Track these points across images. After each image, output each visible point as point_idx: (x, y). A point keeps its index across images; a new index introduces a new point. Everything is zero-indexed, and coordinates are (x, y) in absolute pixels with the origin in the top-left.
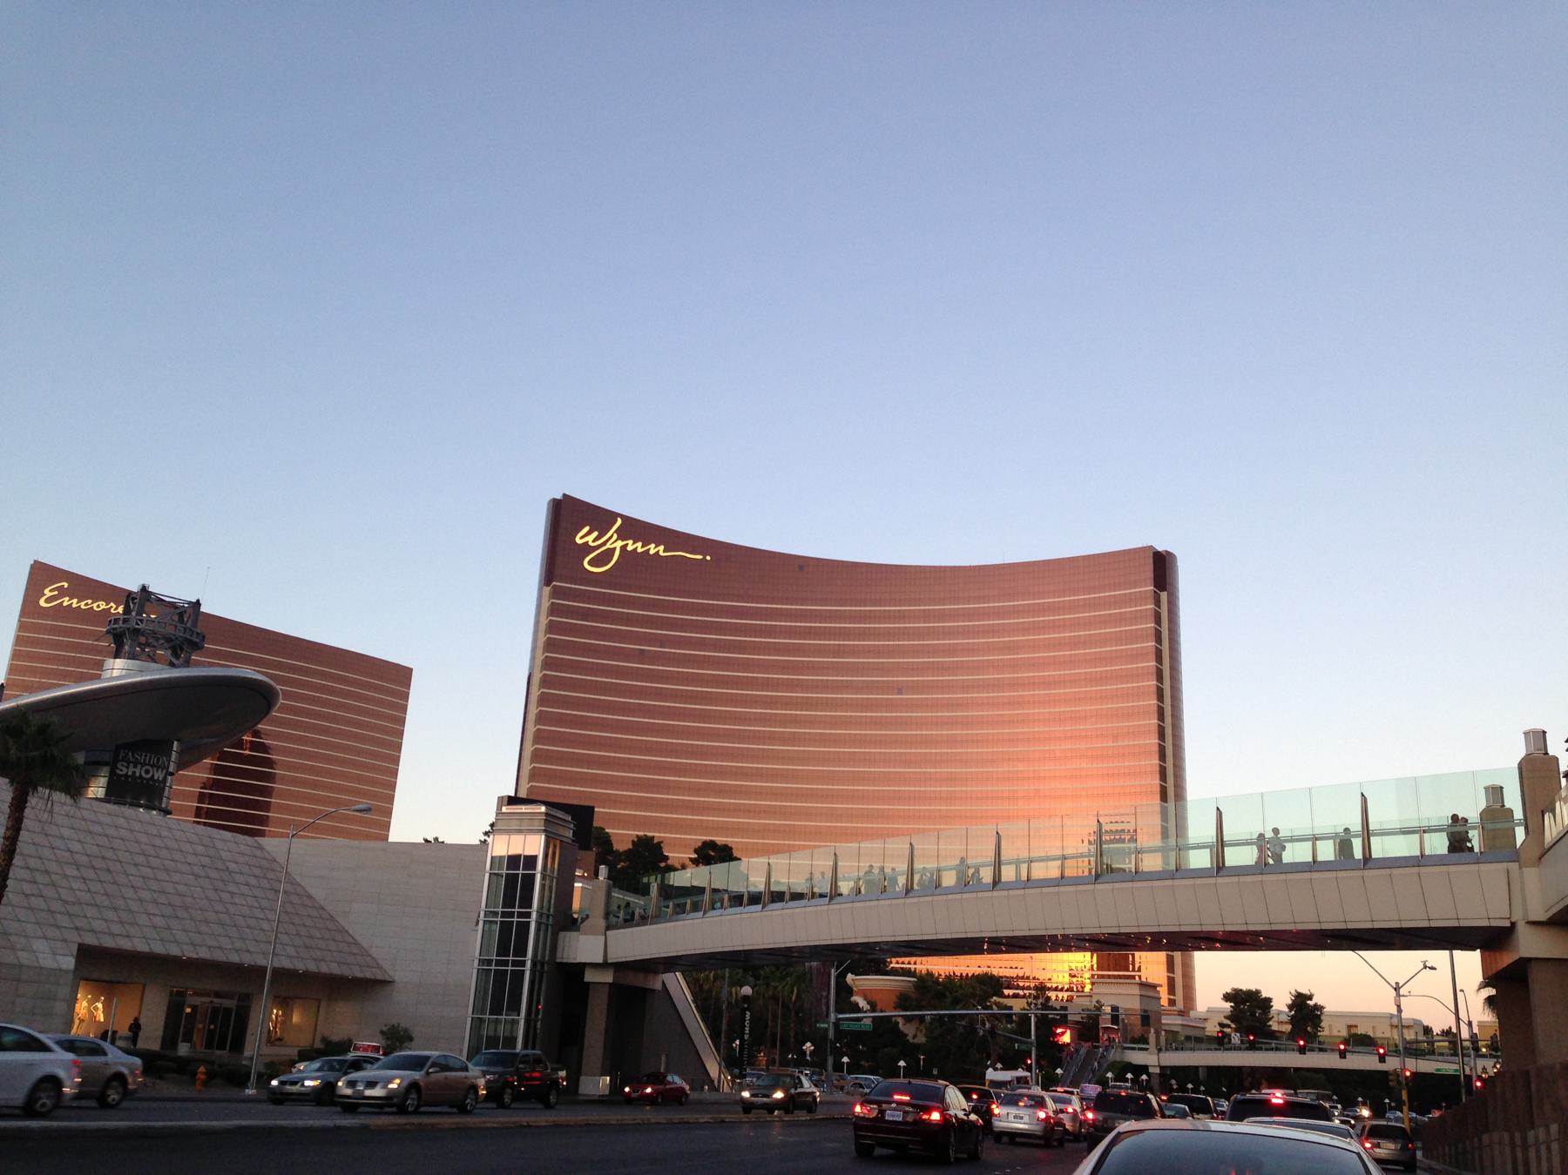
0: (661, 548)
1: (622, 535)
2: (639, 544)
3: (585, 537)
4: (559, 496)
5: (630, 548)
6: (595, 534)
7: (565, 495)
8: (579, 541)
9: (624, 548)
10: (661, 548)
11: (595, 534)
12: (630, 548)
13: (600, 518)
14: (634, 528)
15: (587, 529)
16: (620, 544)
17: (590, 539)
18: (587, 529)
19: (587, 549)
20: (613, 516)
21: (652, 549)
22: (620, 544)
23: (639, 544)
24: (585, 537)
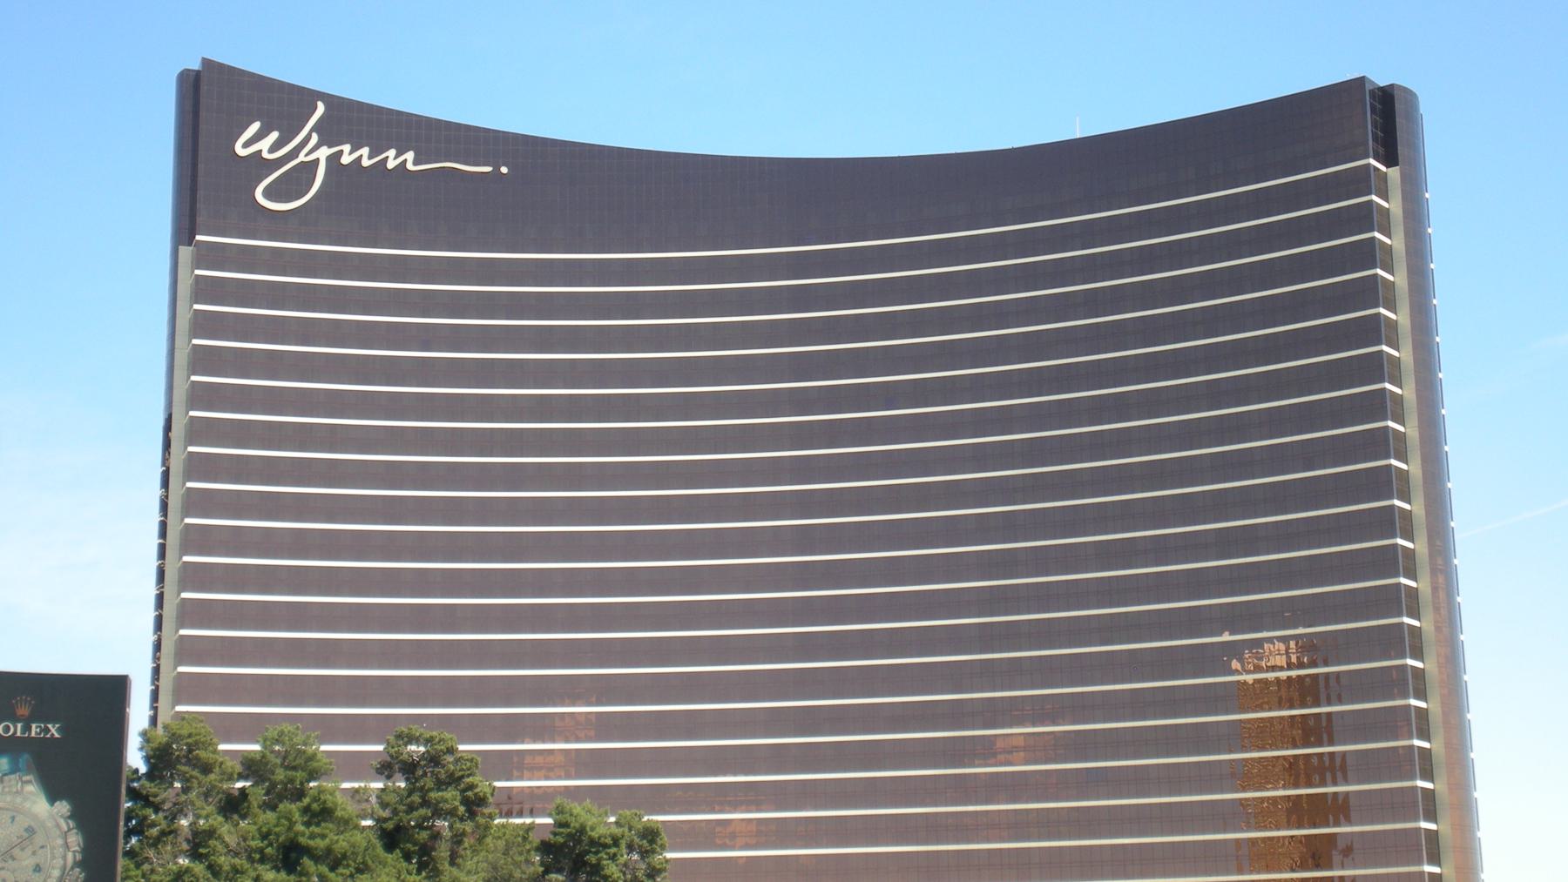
0: (410, 156)
2: (365, 151)
4: (196, 65)
5: (346, 159)
6: (274, 135)
7: (207, 63)
8: (241, 151)
9: (334, 159)
10: (410, 156)
11: (274, 135)
12: (346, 159)
13: (283, 105)
14: (350, 120)
15: (255, 127)
16: (323, 153)
17: (264, 145)
18: (255, 127)
19: (259, 166)
20: (303, 99)
22: (323, 153)
23: (365, 151)
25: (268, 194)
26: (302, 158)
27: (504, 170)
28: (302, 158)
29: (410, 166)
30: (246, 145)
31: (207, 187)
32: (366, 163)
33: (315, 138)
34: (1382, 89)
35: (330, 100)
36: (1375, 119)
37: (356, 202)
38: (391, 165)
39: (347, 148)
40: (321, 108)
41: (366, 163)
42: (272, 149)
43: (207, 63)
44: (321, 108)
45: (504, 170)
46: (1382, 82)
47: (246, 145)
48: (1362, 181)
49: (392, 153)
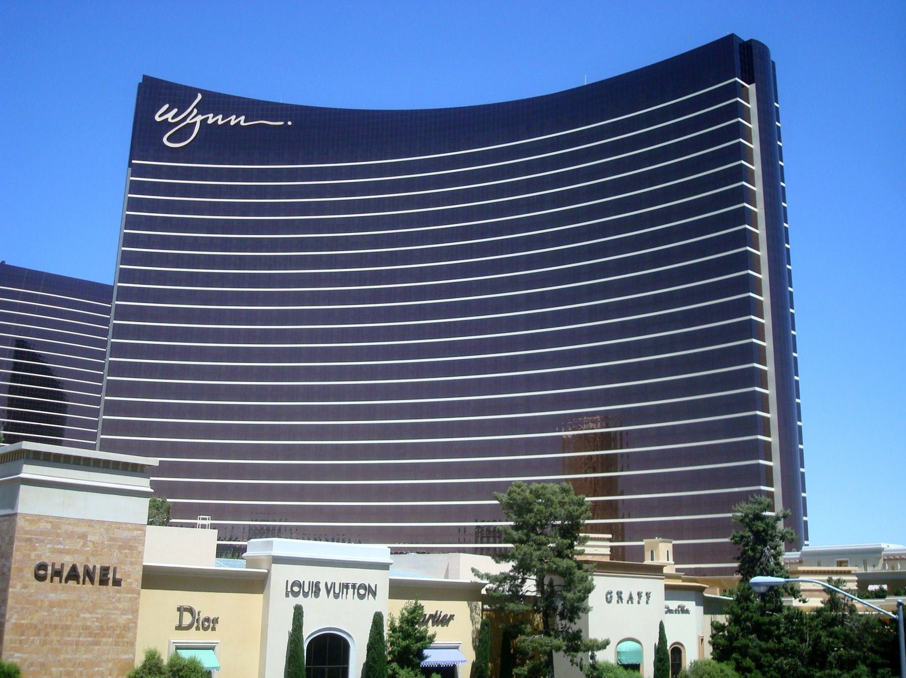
0: (242, 118)
1: (202, 109)
2: (220, 117)
3: (164, 114)
5: (210, 121)
6: (175, 111)
7: (146, 78)
8: (157, 119)
9: (204, 122)
10: (242, 118)
11: (175, 111)
13: (180, 96)
14: (214, 102)
15: (167, 106)
16: (200, 118)
17: (169, 116)
18: (167, 106)
19: (166, 125)
20: (191, 93)
21: (233, 121)
22: (200, 118)
23: (220, 117)
24: (164, 114)
25: (169, 139)
26: (188, 121)
27: (290, 123)
28: (188, 121)
29: (242, 123)
30: (160, 116)
31: (146, 137)
32: (220, 122)
33: (195, 111)
34: (747, 42)
35: (205, 93)
36: (740, 59)
37: (214, 142)
38: (232, 123)
39: (211, 115)
40: (200, 96)
41: (220, 122)
42: (173, 118)
43: (146, 78)
44: (200, 96)
45: (290, 123)
46: (745, 38)
47: (161, 116)
48: (735, 90)
49: (234, 117)
